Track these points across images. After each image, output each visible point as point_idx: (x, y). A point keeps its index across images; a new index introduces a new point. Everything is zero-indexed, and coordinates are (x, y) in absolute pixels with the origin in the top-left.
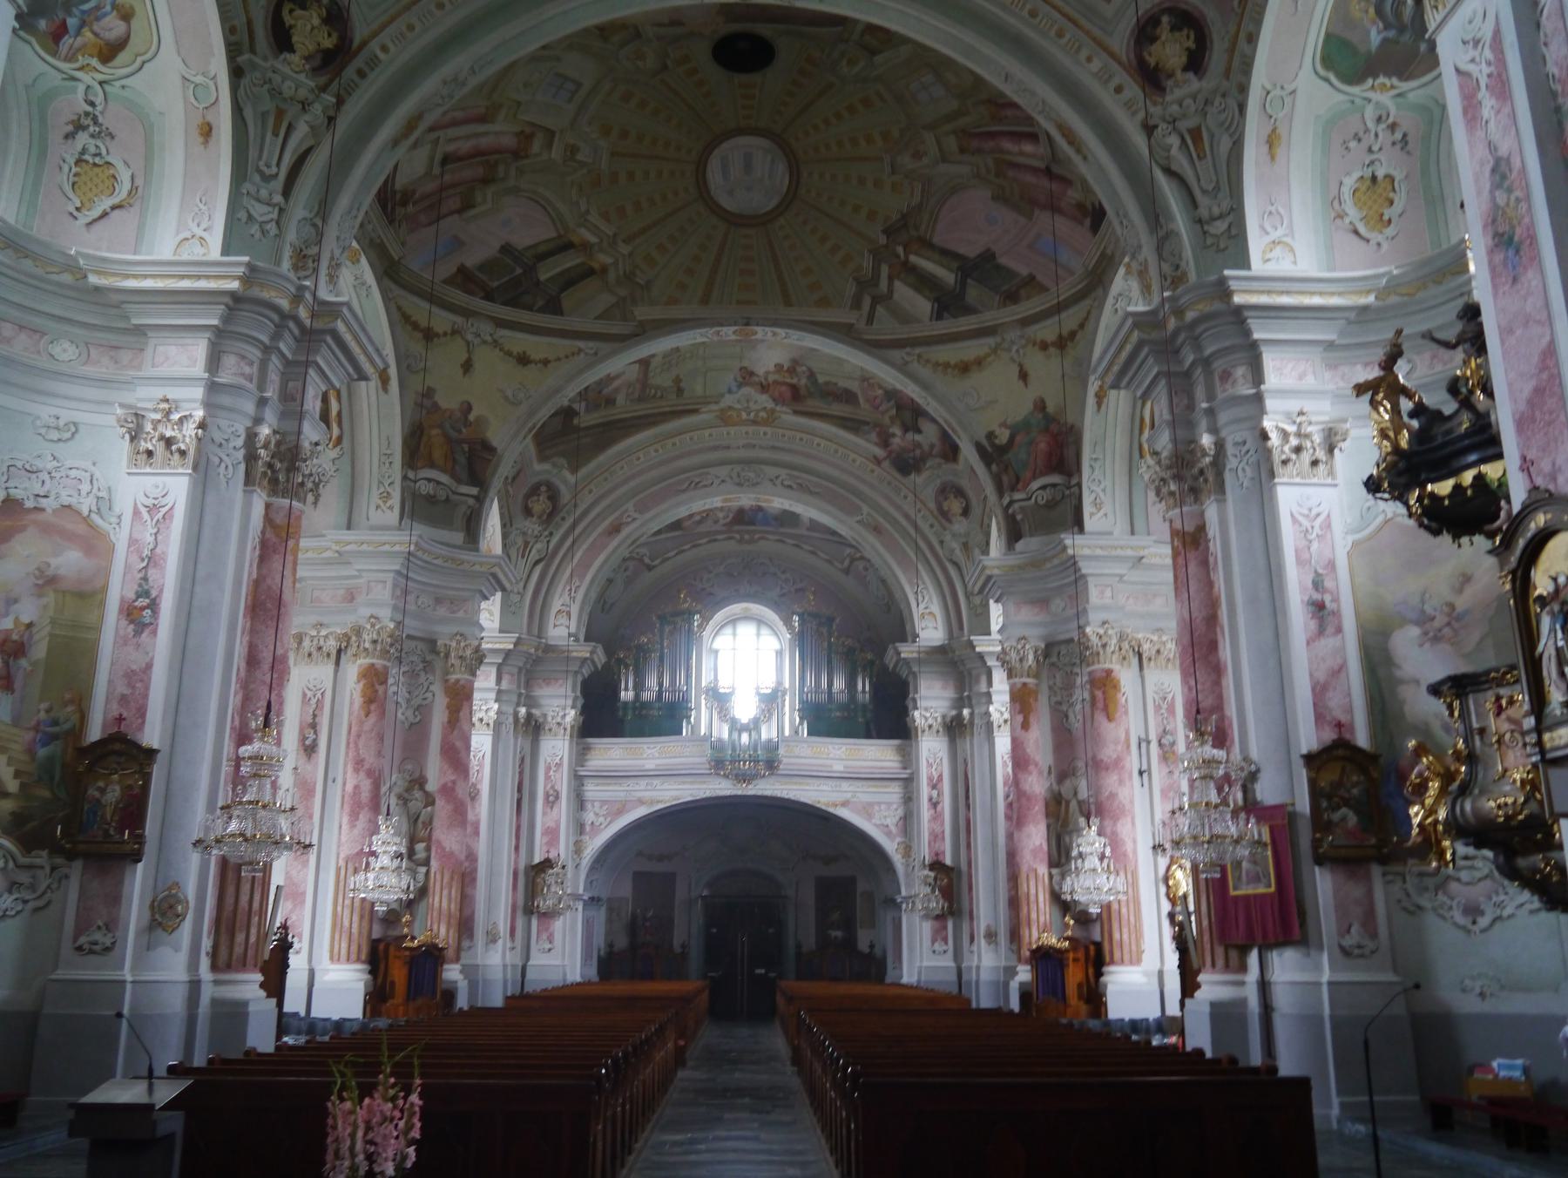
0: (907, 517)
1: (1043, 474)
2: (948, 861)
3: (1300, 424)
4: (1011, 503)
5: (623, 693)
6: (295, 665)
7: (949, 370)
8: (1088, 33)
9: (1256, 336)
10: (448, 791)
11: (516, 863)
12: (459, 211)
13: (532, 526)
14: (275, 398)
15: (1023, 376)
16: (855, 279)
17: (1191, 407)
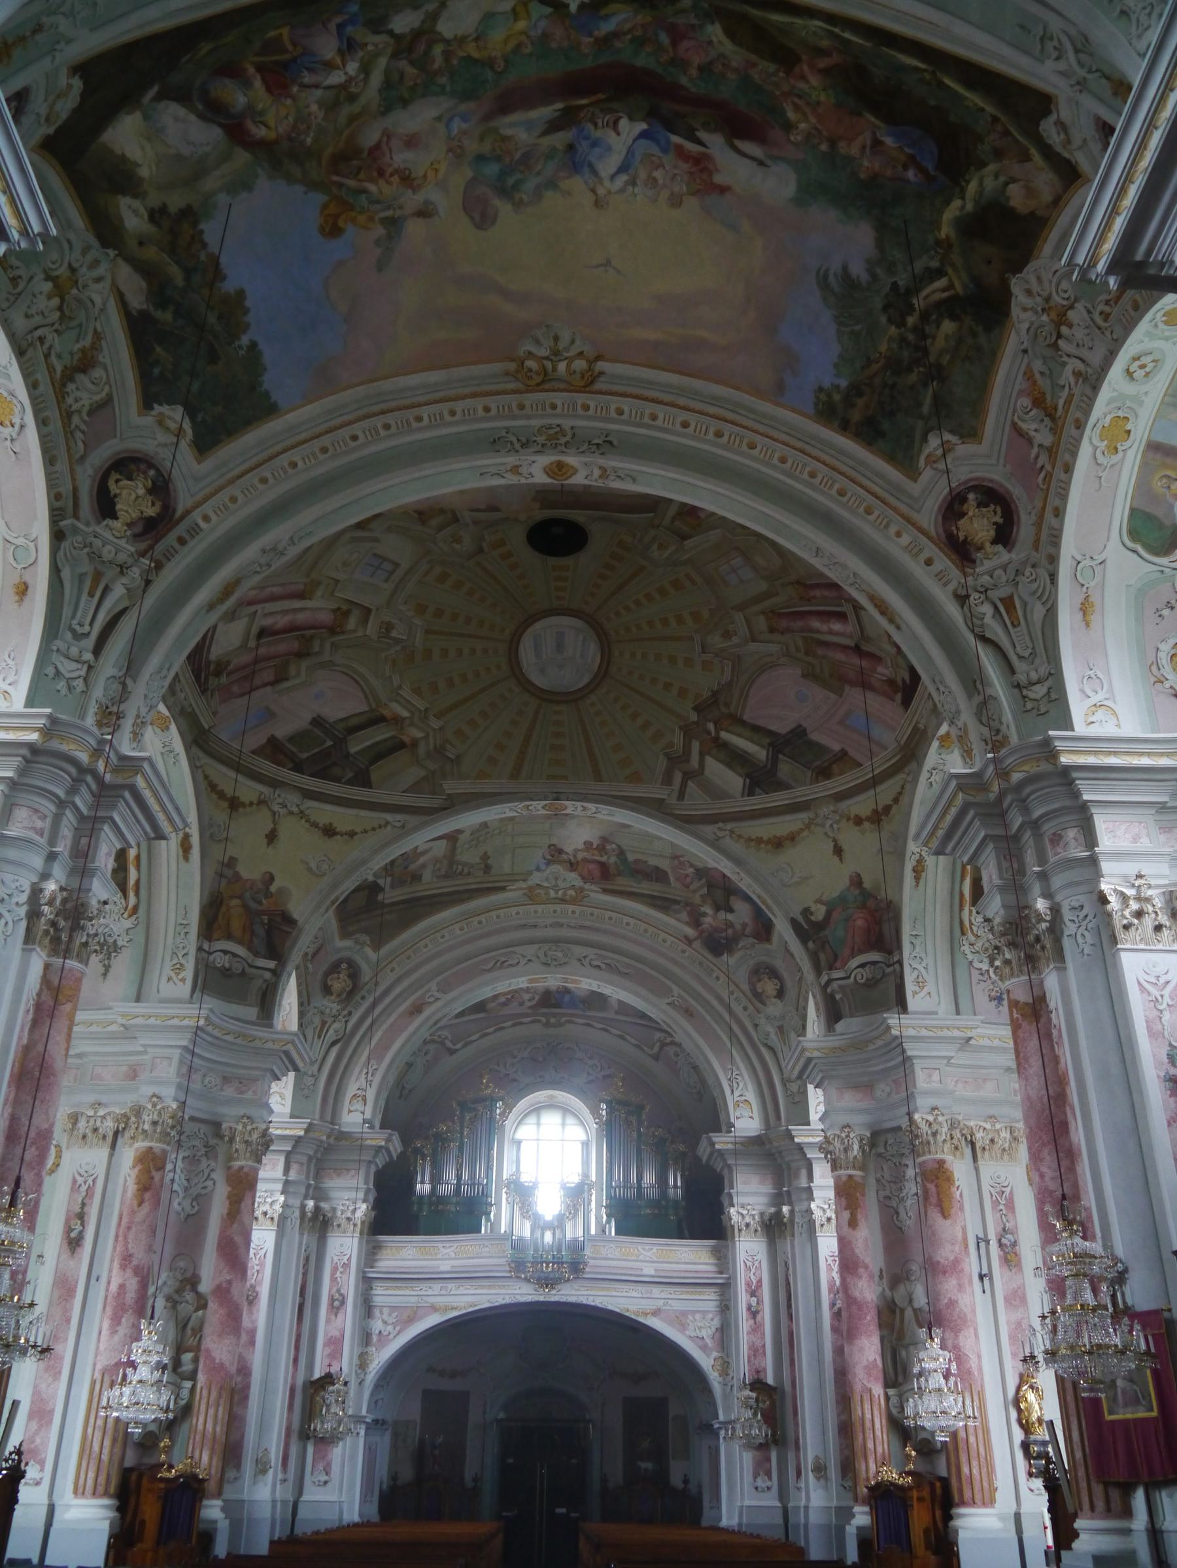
0: (719, 998)
1: (861, 952)
2: (770, 1380)
3: (1139, 886)
4: (830, 981)
5: (418, 1186)
6: (68, 1148)
7: (763, 846)
8: (895, 510)
9: (1086, 797)
10: (222, 1292)
11: (294, 1378)
12: (272, 684)
13: (331, 1005)
14: (66, 854)
15: (838, 851)
16: (666, 755)
17: (1022, 871)
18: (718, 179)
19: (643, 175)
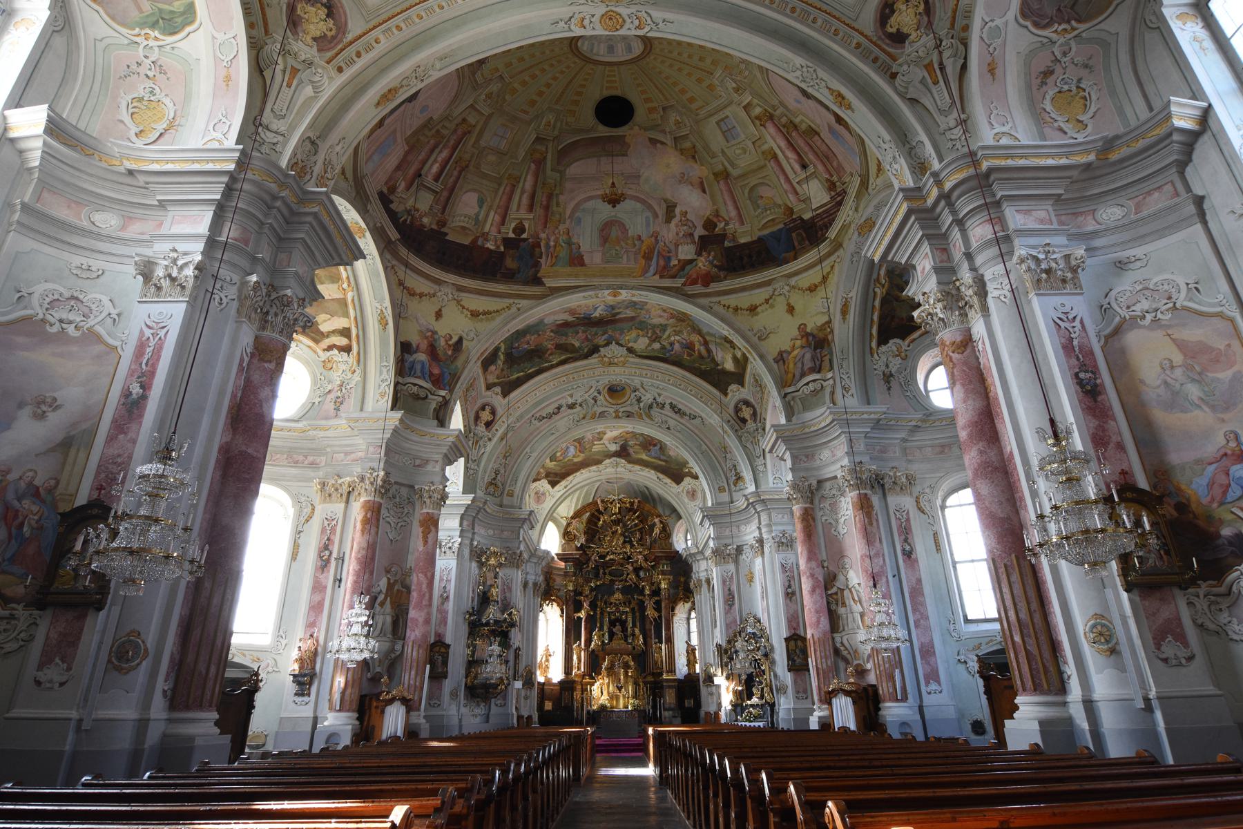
12: (817, 133)
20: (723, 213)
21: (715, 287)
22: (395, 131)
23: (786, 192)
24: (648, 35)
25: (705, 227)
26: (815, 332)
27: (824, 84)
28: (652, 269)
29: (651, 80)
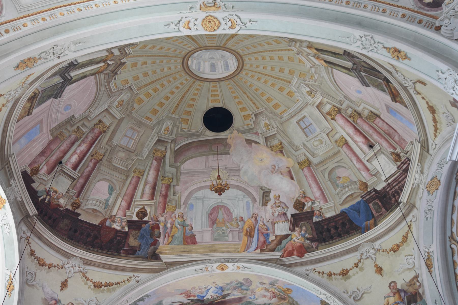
12: (378, 116)
18: (184, 295)
19: (203, 290)
20: (309, 194)
21: (308, 257)
22: (41, 122)
23: (359, 170)
24: (239, 33)
25: (295, 207)
26: (406, 288)
27: (381, 46)
28: (254, 245)
29: (245, 93)
